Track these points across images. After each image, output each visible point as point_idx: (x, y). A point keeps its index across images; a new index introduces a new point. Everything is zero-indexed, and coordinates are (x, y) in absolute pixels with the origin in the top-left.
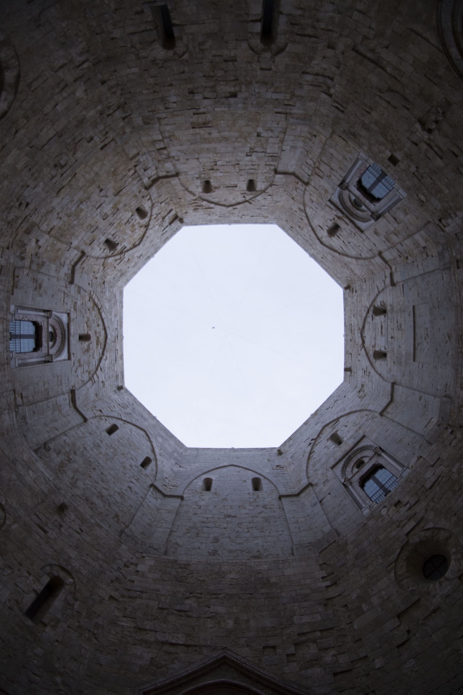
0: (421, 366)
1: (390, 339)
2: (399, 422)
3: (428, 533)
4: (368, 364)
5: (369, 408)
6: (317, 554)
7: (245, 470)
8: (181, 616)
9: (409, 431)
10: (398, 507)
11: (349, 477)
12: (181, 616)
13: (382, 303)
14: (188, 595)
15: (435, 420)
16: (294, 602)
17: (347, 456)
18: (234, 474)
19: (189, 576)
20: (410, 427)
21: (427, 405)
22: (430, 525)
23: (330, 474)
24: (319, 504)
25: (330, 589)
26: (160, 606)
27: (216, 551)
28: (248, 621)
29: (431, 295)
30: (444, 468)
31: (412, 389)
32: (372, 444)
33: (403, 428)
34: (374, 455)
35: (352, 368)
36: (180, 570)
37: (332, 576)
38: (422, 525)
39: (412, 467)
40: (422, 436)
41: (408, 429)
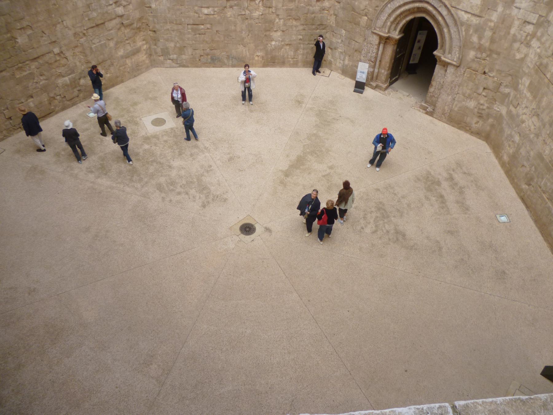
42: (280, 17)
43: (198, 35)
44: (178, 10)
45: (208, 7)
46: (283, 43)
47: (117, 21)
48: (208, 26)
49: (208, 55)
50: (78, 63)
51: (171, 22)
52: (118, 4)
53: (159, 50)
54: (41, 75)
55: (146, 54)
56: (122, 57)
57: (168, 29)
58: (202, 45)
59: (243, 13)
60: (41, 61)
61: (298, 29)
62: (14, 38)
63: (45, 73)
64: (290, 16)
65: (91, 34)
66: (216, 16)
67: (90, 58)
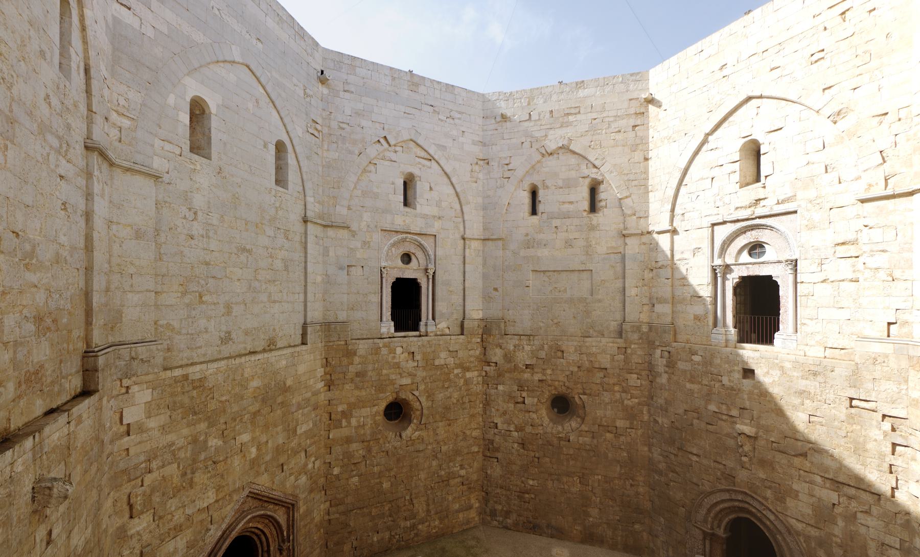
1: (556, 222)
4: (520, 173)
5: (465, 209)
7: (268, 100)
13: (603, 204)
17: (404, 236)
18: (250, 106)
23: (377, 237)
29: (600, 301)
35: (508, 123)
36: (194, 393)
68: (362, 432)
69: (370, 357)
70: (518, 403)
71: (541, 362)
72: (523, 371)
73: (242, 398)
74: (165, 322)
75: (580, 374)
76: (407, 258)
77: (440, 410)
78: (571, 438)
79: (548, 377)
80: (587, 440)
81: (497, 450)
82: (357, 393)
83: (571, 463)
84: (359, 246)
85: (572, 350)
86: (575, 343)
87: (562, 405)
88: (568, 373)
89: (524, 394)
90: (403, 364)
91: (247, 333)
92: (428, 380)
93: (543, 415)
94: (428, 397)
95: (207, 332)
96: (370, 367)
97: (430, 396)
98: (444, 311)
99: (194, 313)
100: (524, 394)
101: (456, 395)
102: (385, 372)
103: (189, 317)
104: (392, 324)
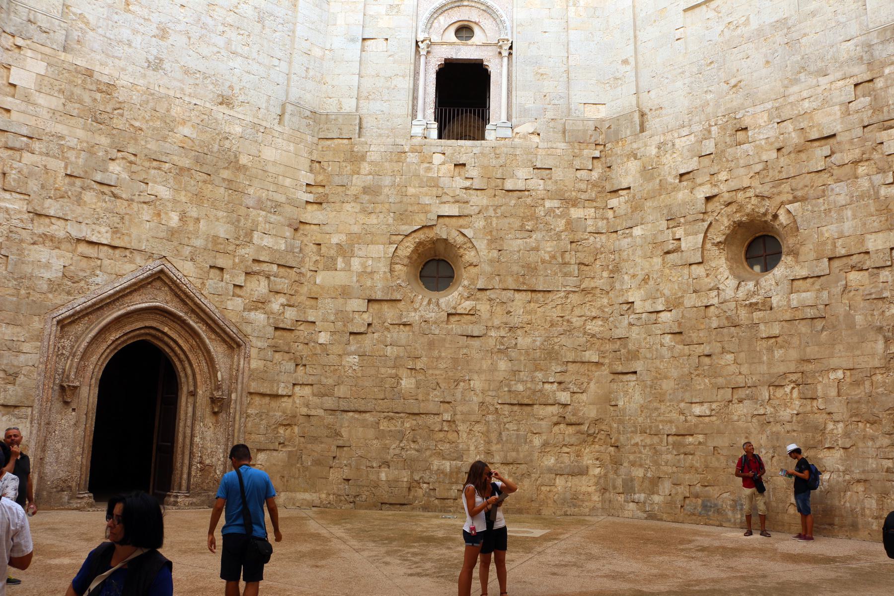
0: (678, 34)
2: (571, 45)
3: (460, 240)
6: (315, 140)
8: (103, 193)
9: (565, 75)
10: (457, 169)
11: (435, 38)
12: (103, 193)
14: (114, 153)
15: (602, 113)
16: (261, 209)
19: (116, 112)
20: (572, 75)
21: (620, 82)
22: (469, 233)
24: (359, 44)
25: (309, 207)
26: (69, 173)
27: (161, 60)
28: (198, 220)
30: (541, 187)
31: (635, 31)
32: (508, 24)
33: (565, 60)
34: (496, 45)
36: (98, 96)
37: (320, 190)
38: (461, 221)
39: (517, 133)
40: (570, 109)
41: (567, 72)
42: (835, 417)
43: (682, 456)
44: (656, 409)
45: (701, 403)
46: (847, 477)
47: (554, 409)
48: (701, 438)
49: (697, 496)
50: (472, 448)
51: (643, 432)
52: (563, 386)
53: (619, 482)
54: (414, 442)
55: (596, 484)
56: (550, 470)
57: (637, 444)
58: (687, 476)
59: (762, 412)
60: (420, 420)
61: (878, 444)
62: (398, 378)
63: (420, 440)
64: (856, 415)
65: (506, 413)
66: (714, 418)
67: (494, 448)
68: (369, 283)
69: (387, 164)
70: (668, 253)
71: (706, 161)
72: (675, 189)
73: (165, 139)
74: (79, 12)
75: (783, 161)
76: (464, 31)
77: (515, 268)
78: (775, 301)
79: (723, 187)
80: (808, 297)
81: (634, 355)
82: (362, 218)
83: (778, 353)
84: (384, 12)
85: (762, 119)
86: (769, 105)
87: (759, 244)
88: (758, 167)
89: (679, 232)
90: (445, 182)
91: (186, 71)
92: (491, 212)
93: (726, 281)
94: (491, 242)
95: (130, 45)
96: (387, 181)
97: (496, 241)
98: (530, 105)
99: (116, 17)
100: (679, 232)
101: (549, 247)
102: (411, 190)
103: (108, 18)
104: (435, 125)
